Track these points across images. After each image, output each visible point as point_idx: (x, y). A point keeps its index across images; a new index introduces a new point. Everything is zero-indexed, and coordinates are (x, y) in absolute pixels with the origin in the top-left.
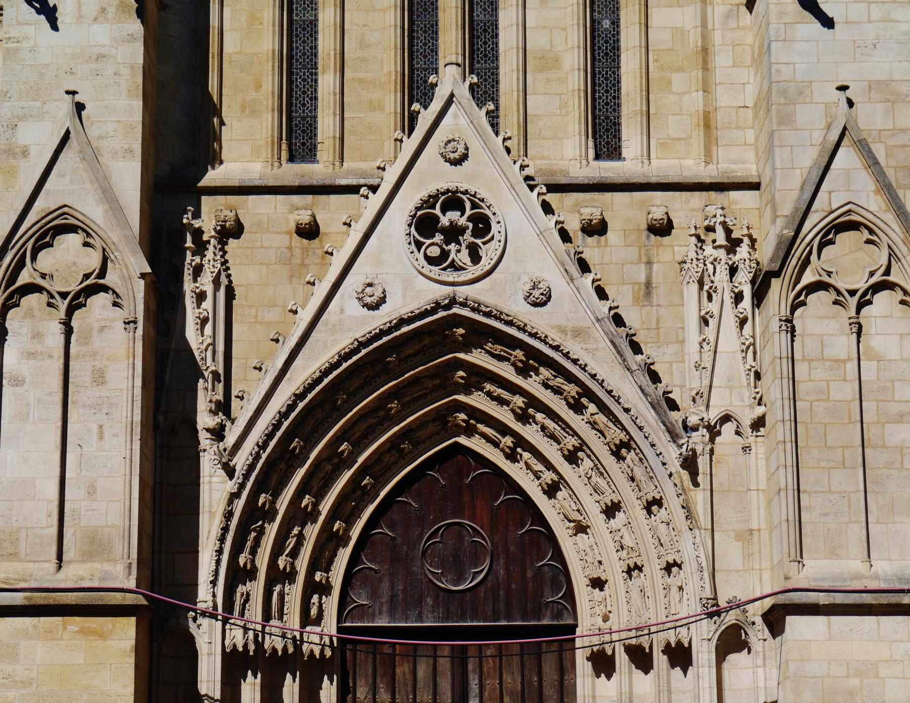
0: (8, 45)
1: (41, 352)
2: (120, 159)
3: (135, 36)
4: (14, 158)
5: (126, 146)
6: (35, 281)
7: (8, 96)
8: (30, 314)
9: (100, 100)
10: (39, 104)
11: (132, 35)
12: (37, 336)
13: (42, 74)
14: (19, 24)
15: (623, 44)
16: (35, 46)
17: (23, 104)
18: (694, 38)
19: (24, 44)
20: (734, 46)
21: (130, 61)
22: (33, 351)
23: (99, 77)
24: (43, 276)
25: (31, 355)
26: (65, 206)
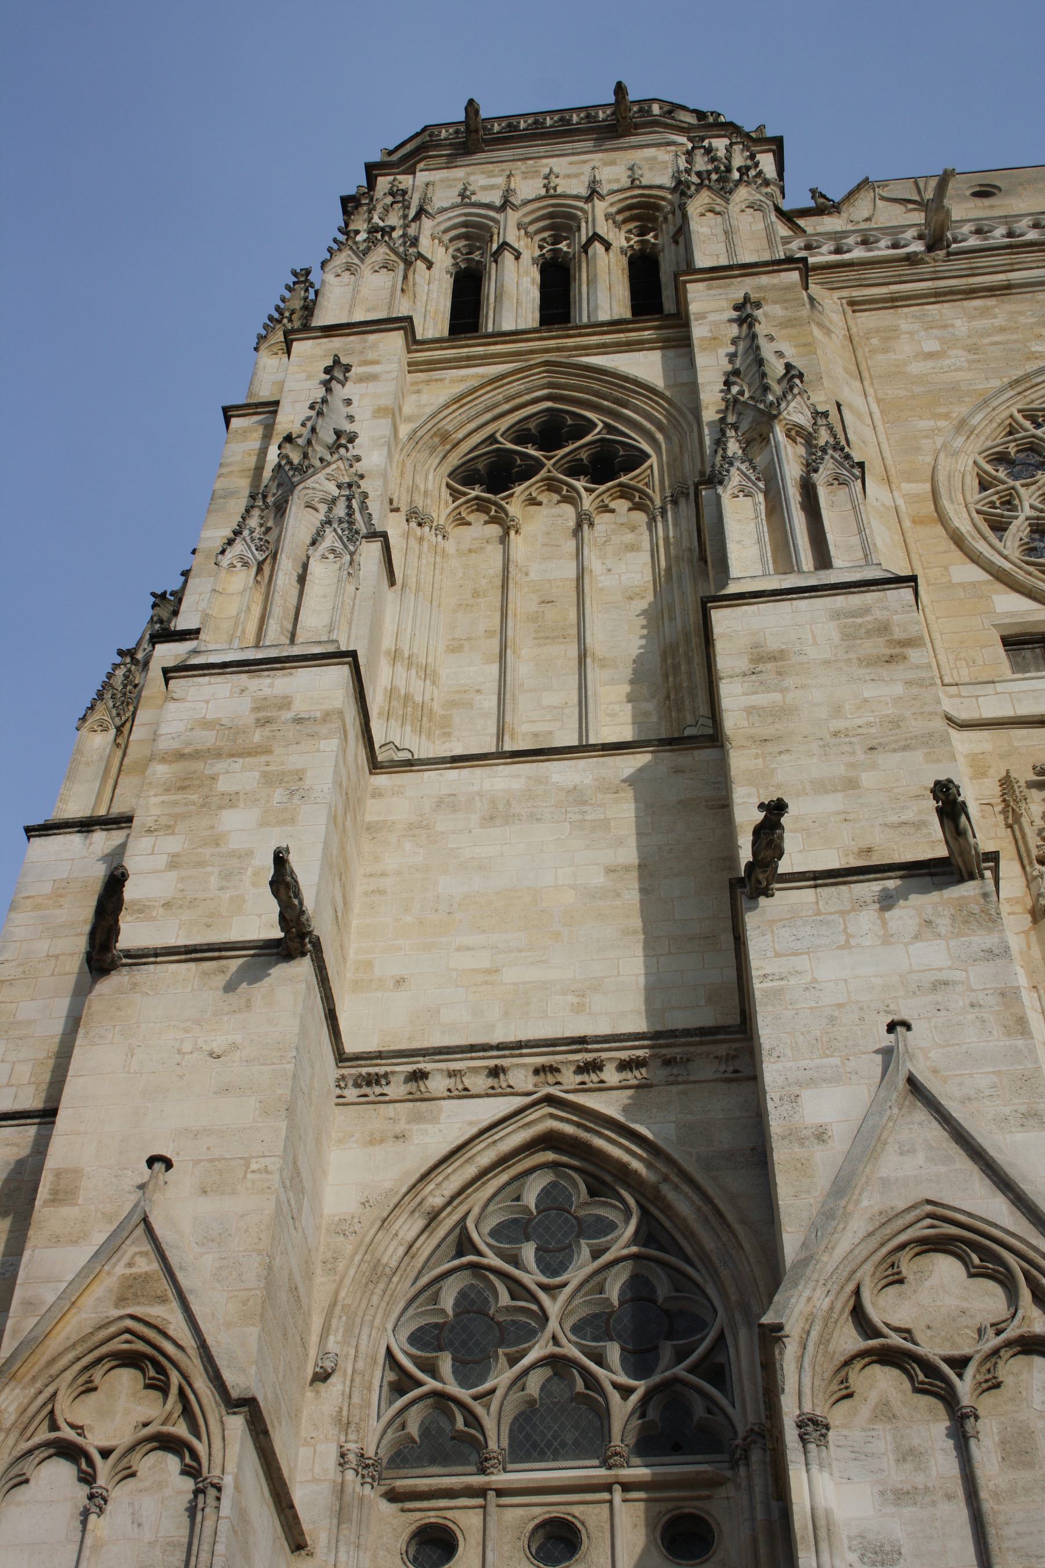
0: (764, 985)
1: (926, 1488)
2: (1013, 1129)
3: (996, 951)
4: (802, 1145)
5: (1023, 1109)
6: (889, 1341)
7: (775, 1054)
8: (884, 1412)
9: (953, 1045)
10: (835, 1061)
12: (908, 1455)
13: (832, 1019)
14: (777, 955)
16: (814, 980)
17: (804, 1063)
19: (793, 981)
21: (995, 986)
22: (907, 1487)
23: (943, 1013)
24: (906, 1333)
25: (901, 1496)
26: (929, 1202)
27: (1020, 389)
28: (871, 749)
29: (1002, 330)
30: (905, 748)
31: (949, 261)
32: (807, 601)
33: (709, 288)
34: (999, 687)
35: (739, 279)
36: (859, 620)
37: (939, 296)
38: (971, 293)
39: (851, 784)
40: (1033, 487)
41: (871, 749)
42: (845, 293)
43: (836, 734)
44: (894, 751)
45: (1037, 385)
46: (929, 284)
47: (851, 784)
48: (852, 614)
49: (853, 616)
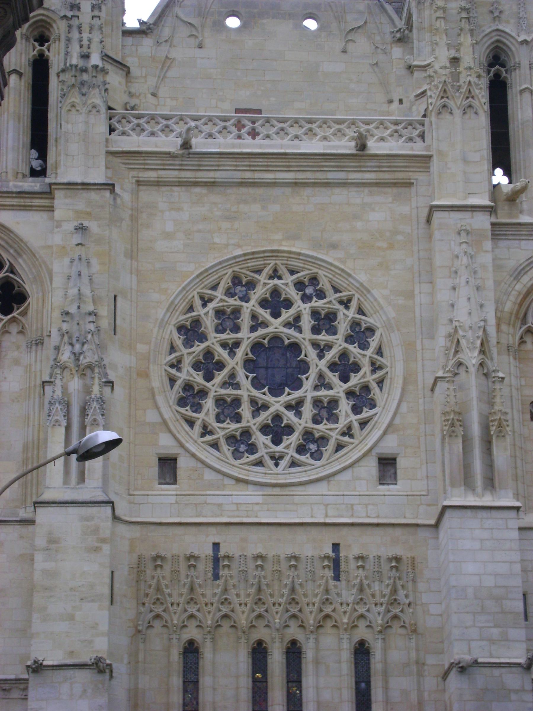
11: (100, 706)
15: (373, 698)
18: (414, 697)
20: (436, 701)
27: (201, 278)
28: (81, 599)
29: (205, 219)
30: (93, 601)
31: (189, 157)
32: (72, 508)
33: (66, 197)
34: (151, 499)
35: (81, 191)
36: (89, 523)
37: (181, 184)
38: (196, 184)
39: (71, 618)
40: (194, 355)
41: (81, 599)
42: (135, 173)
43: (71, 589)
44: (89, 602)
45: (210, 274)
46: (176, 173)
47: (71, 618)
48: (87, 519)
49: (88, 521)
